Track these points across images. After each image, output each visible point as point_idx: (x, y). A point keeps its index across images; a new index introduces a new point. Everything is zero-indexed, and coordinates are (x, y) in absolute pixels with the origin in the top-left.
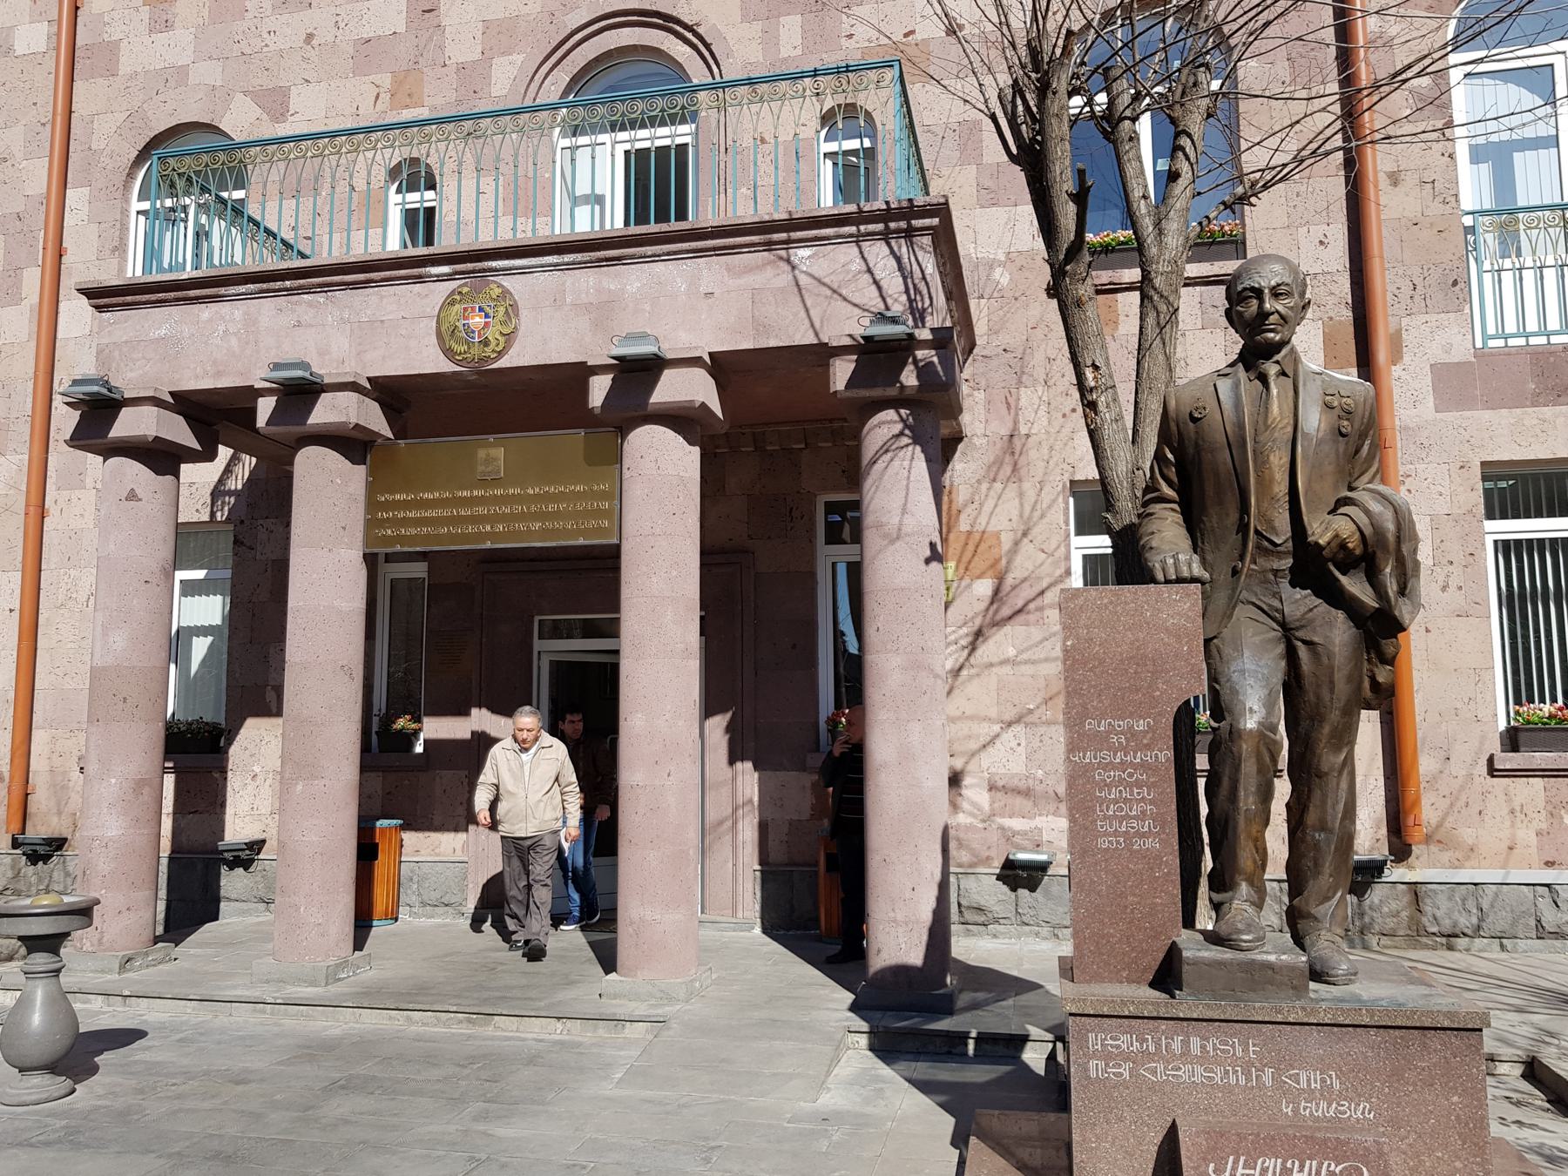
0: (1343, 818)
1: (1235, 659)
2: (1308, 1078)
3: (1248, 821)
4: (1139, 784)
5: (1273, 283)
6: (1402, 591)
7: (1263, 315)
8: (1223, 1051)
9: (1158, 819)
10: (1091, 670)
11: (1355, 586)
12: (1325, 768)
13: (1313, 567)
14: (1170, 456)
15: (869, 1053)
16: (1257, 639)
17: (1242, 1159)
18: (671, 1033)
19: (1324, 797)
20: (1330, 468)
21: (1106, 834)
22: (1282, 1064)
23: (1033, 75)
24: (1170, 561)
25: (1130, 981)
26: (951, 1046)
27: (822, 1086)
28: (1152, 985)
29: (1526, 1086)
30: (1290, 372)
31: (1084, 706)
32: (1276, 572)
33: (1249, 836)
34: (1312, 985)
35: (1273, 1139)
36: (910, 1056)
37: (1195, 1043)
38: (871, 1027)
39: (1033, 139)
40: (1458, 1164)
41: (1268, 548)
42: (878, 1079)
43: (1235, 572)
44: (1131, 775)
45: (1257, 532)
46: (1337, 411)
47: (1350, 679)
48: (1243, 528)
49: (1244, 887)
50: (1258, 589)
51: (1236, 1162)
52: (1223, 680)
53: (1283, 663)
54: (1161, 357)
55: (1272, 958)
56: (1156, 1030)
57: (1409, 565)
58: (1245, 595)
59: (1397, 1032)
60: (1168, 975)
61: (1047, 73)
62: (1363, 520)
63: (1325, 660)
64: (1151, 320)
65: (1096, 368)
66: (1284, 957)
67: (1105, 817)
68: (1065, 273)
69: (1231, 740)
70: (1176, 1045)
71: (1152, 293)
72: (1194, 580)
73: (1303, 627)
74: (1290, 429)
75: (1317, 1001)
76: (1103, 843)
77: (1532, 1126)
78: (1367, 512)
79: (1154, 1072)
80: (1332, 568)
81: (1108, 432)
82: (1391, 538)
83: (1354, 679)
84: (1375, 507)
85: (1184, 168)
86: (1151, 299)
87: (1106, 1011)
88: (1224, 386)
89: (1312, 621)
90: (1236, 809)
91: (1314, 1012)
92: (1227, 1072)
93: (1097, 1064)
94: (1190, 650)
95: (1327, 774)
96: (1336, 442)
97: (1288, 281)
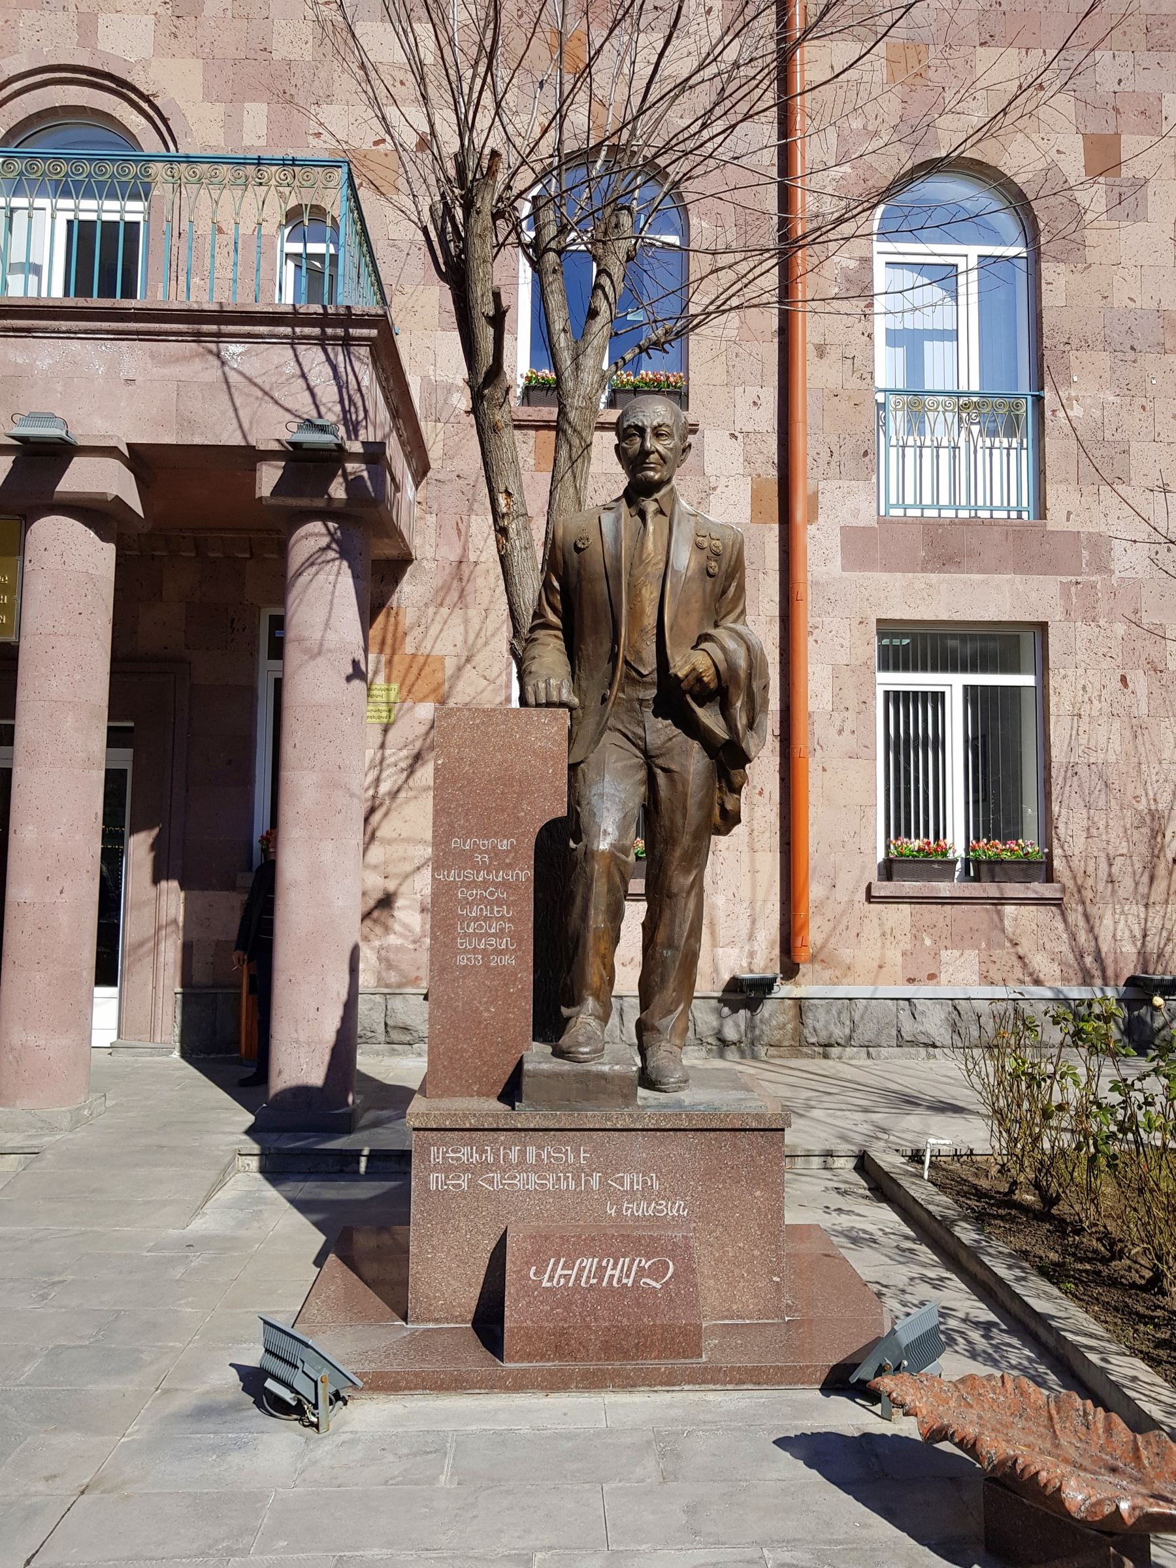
0: (688, 937)
1: (597, 783)
2: (631, 1180)
3: (598, 938)
4: (499, 902)
5: (655, 423)
6: (751, 725)
7: (645, 453)
8: (557, 1159)
9: (515, 937)
10: (459, 789)
11: (709, 717)
12: (675, 889)
13: (674, 699)
14: (556, 584)
15: (259, 1176)
16: (619, 765)
17: (562, 1260)
18: (43, 1164)
19: (674, 916)
20: (696, 605)
21: (465, 951)
22: (610, 1168)
23: (457, 191)
24: (542, 685)
25: (480, 1094)
26: (343, 1165)
27: (198, 1210)
28: (501, 1098)
29: (856, 1178)
30: (667, 511)
31: (451, 824)
32: (641, 702)
33: (597, 952)
34: (642, 1092)
35: (593, 1239)
36: (302, 1177)
37: (531, 1151)
38: (262, 1149)
39: (459, 256)
40: (756, 1253)
41: (635, 678)
42: (262, 1201)
43: (604, 700)
44: (492, 894)
45: (626, 662)
46: (706, 552)
47: (701, 805)
48: (614, 657)
49: (590, 1002)
50: (625, 718)
51: (556, 1263)
52: (584, 803)
53: (643, 789)
54: (572, 490)
55: (606, 1068)
56: (496, 1141)
57: (758, 701)
58: (612, 722)
59: (712, 1134)
60: (511, 1092)
61: (470, 190)
62: (719, 656)
63: (680, 788)
64: (564, 453)
65: (509, 494)
66: (617, 1067)
67: (466, 935)
68: (483, 397)
69: (586, 860)
70: (514, 1155)
71: (566, 426)
72: (562, 705)
73: (662, 755)
74: (662, 565)
75: (644, 1107)
76: (462, 960)
77: (849, 1212)
78: (723, 649)
79: (491, 1182)
80: (689, 699)
81: (518, 559)
82: (742, 674)
83: (706, 806)
84: (731, 644)
85: (603, 306)
86: (564, 432)
87: (448, 1124)
88: (608, 519)
89: (670, 750)
90: (587, 927)
91: (640, 1118)
92: (559, 1179)
93: (436, 1175)
94: (555, 773)
95: (676, 895)
96: (704, 581)
97: (669, 422)
